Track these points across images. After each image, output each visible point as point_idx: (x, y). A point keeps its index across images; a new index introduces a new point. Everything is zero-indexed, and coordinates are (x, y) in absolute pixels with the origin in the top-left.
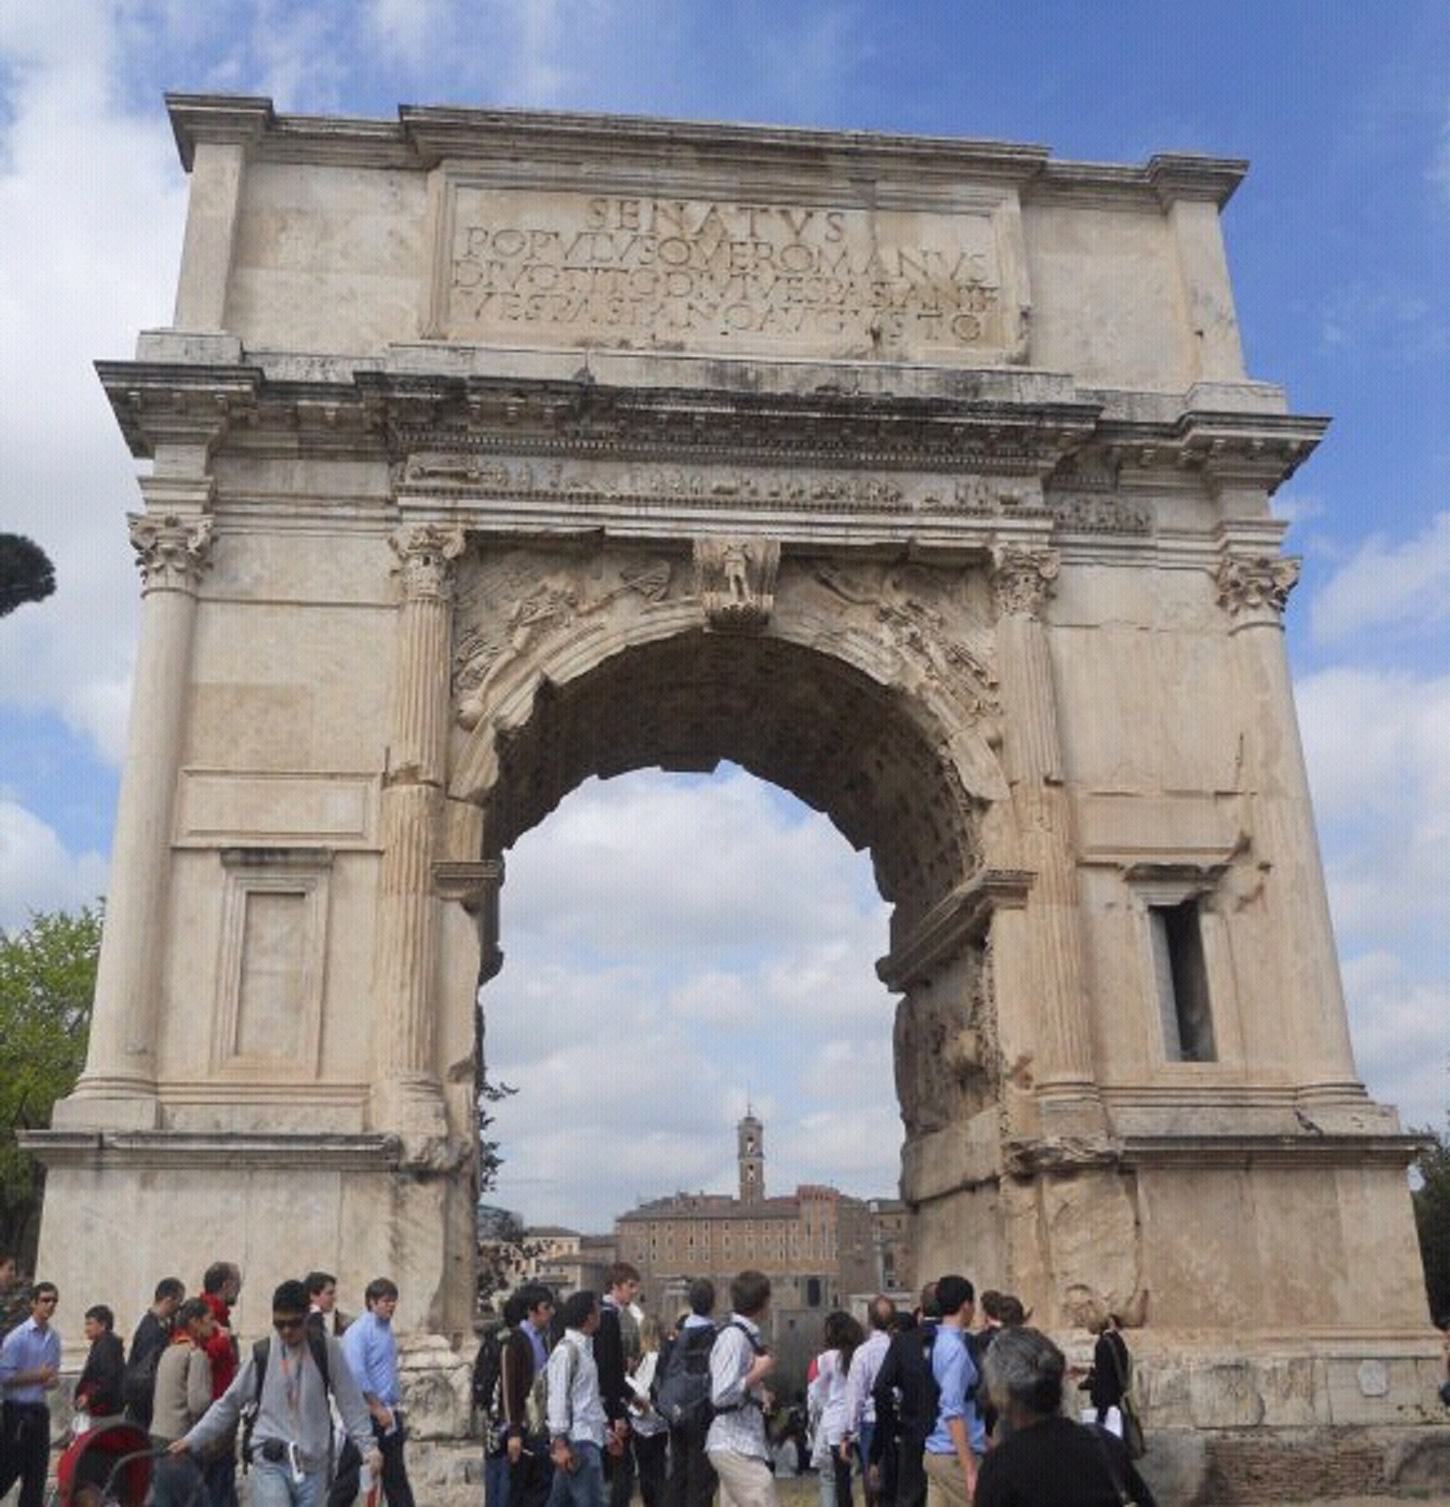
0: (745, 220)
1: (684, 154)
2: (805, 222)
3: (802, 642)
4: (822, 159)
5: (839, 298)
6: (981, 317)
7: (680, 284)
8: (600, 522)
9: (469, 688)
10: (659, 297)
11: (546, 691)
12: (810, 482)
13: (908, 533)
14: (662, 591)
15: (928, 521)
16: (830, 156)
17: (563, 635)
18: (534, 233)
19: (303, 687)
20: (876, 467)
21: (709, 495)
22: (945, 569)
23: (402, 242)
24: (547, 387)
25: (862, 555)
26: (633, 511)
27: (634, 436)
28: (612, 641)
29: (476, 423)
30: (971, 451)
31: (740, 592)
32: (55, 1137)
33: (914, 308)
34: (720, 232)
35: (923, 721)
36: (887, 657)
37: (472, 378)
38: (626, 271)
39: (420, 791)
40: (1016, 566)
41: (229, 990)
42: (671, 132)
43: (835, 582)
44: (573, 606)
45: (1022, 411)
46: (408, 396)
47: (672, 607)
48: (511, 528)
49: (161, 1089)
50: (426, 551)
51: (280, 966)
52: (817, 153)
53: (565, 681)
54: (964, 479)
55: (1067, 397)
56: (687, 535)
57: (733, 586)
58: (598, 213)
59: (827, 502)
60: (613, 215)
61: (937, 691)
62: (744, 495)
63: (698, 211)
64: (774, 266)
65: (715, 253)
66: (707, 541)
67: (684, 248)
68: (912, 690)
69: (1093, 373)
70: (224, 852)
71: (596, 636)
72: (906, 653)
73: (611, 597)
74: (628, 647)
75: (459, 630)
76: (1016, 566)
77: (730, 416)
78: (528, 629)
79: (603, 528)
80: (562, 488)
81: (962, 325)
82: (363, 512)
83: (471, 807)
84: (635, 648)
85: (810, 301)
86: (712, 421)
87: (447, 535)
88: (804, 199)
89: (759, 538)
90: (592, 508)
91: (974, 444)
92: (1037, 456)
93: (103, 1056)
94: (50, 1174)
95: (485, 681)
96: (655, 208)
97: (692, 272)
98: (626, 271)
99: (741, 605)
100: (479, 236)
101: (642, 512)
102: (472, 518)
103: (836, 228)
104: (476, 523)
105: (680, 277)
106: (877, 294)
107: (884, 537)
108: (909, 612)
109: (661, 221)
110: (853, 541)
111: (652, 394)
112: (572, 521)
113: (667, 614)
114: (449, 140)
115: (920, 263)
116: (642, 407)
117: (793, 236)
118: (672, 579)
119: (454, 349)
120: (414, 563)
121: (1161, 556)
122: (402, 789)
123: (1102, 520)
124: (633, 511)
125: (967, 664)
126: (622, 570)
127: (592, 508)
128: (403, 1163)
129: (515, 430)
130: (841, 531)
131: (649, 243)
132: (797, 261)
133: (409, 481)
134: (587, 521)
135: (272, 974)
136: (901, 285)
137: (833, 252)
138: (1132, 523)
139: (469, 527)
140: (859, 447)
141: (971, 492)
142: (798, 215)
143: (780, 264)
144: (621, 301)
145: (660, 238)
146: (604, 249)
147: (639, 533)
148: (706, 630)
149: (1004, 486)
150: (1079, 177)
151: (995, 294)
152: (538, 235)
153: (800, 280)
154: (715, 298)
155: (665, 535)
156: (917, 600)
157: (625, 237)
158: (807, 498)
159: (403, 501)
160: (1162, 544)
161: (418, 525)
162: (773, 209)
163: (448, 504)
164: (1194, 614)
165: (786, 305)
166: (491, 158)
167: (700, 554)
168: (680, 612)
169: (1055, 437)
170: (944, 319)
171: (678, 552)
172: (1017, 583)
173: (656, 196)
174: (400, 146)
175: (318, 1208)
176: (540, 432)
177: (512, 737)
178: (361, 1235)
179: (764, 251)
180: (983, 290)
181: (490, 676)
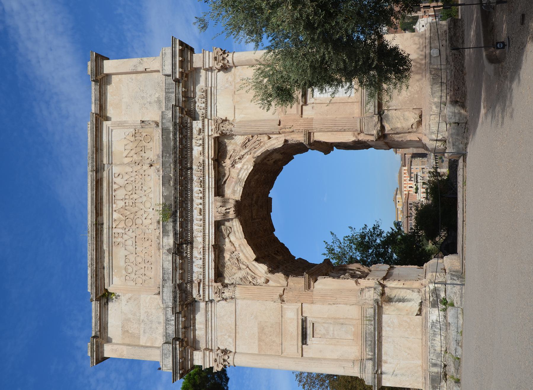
0: (118, 202)
1: (100, 220)
2: (118, 184)
3: (242, 190)
4: (99, 180)
5: (141, 177)
6: (144, 134)
7: (139, 221)
8: (210, 246)
10: (143, 227)
11: (256, 260)
12: (196, 188)
13: (210, 160)
15: (206, 155)
16: (98, 179)
17: (242, 256)
18: (126, 262)
19: (258, 324)
20: (191, 168)
21: (201, 217)
22: (219, 149)
23: (129, 299)
24: (174, 262)
25: (217, 171)
26: (207, 237)
27: (186, 237)
29: (184, 281)
30: (186, 142)
31: (229, 209)
32: (374, 385)
33: (142, 154)
34: (122, 210)
35: (262, 157)
36: (245, 167)
37: (173, 283)
38: (136, 237)
39: (286, 295)
40: (219, 130)
41: (338, 342)
42: (93, 225)
44: (233, 252)
45: (175, 129)
46: (178, 299)
48: (213, 270)
49: (362, 358)
50: (220, 293)
51: (332, 329)
52: (97, 182)
54: (194, 144)
55: (169, 114)
56: (213, 222)
57: (228, 211)
58: (118, 244)
59: (202, 183)
60: (119, 240)
61: (254, 153)
62: (201, 207)
63: (116, 216)
64: (132, 194)
65: (129, 211)
66: (215, 217)
67: (127, 220)
69: (159, 101)
70: (303, 344)
71: (242, 247)
72: (244, 160)
73: (231, 241)
75: (241, 283)
76: (219, 130)
77: (179, 211)
78: (241, 265)
80: (202, 257)
81: (147, 140)
82: (210, 309)
83: (289, 280)
84: (245, 235)
85: (142, 184)
86: (181, 216)
87: (216, 288)
88: (111, 185)
89: (213, 203)
90: (207, 248)
91: (184, 142)
92: (187, 123)
93: (353, 371)
94: (383, 385)
95: (255, 276)
96: (115, 228)
97: (135, 218)
98: (136, 237)
100: (127, 278)
101: (207, 234)
102: (210, 281)
103: (119, 175)
104: (212, 279)
105: (137, 221)
106: (138, 164)
107: (211, 167)
108: (232, 159)
109: (119, 226)
110: (213, 176)
111: (175, 234)
112: (210, 254)
114: (100, 287)
115: (129, 151)
116: (178, 236)
117: (122, 188)
119: (163, 287)
120: (223, 296)
121: (213, 86)
122: (285, 297)
123: (204, 103)
124: (207, 237)
125: (247, 143)
127: (207, 248)
128: (380, 300)
129: (186, 270)
130: (210, 179)
131: (127, 230)
132: (130, 188)
133: (201, 298)
134: (210, 250)
135: (333, 330)
136: (135, 157)
137: (126, 177)
138: (204, 94)
140: (187, 174)
141: (198, 142)
142: (115, 187)
143: (131, 192)
144: (145, 238)
145: (125, 227)
146: (129, 242)
147: (213, 236)
149: (195, 132)
150: (98, 103)
151: (137, 130)
152: (126, 261)
153: (135, 187)
154: (143, 211)
155: (213, 228)
156: (228, 156)
157: (125, 237)
158: (201, 189)
159: (207, 299)
160: (210, 86)
161: (213, 295)
162: (114, 194)
163: (207, 287)
164: (230, 77)
165: (143, 191)
166: (104, 275)
167: (219, 219)
169: (181, 118)
170: (145, 145)
171: (218, 225)
172: (223, 130)
173: (112, 228)
174: (102, 300)
175: (391, 320)
176: (186, 263)
178: (398, 309)
179: (127, 197)
180: (135, 133)
181: (253, 275)
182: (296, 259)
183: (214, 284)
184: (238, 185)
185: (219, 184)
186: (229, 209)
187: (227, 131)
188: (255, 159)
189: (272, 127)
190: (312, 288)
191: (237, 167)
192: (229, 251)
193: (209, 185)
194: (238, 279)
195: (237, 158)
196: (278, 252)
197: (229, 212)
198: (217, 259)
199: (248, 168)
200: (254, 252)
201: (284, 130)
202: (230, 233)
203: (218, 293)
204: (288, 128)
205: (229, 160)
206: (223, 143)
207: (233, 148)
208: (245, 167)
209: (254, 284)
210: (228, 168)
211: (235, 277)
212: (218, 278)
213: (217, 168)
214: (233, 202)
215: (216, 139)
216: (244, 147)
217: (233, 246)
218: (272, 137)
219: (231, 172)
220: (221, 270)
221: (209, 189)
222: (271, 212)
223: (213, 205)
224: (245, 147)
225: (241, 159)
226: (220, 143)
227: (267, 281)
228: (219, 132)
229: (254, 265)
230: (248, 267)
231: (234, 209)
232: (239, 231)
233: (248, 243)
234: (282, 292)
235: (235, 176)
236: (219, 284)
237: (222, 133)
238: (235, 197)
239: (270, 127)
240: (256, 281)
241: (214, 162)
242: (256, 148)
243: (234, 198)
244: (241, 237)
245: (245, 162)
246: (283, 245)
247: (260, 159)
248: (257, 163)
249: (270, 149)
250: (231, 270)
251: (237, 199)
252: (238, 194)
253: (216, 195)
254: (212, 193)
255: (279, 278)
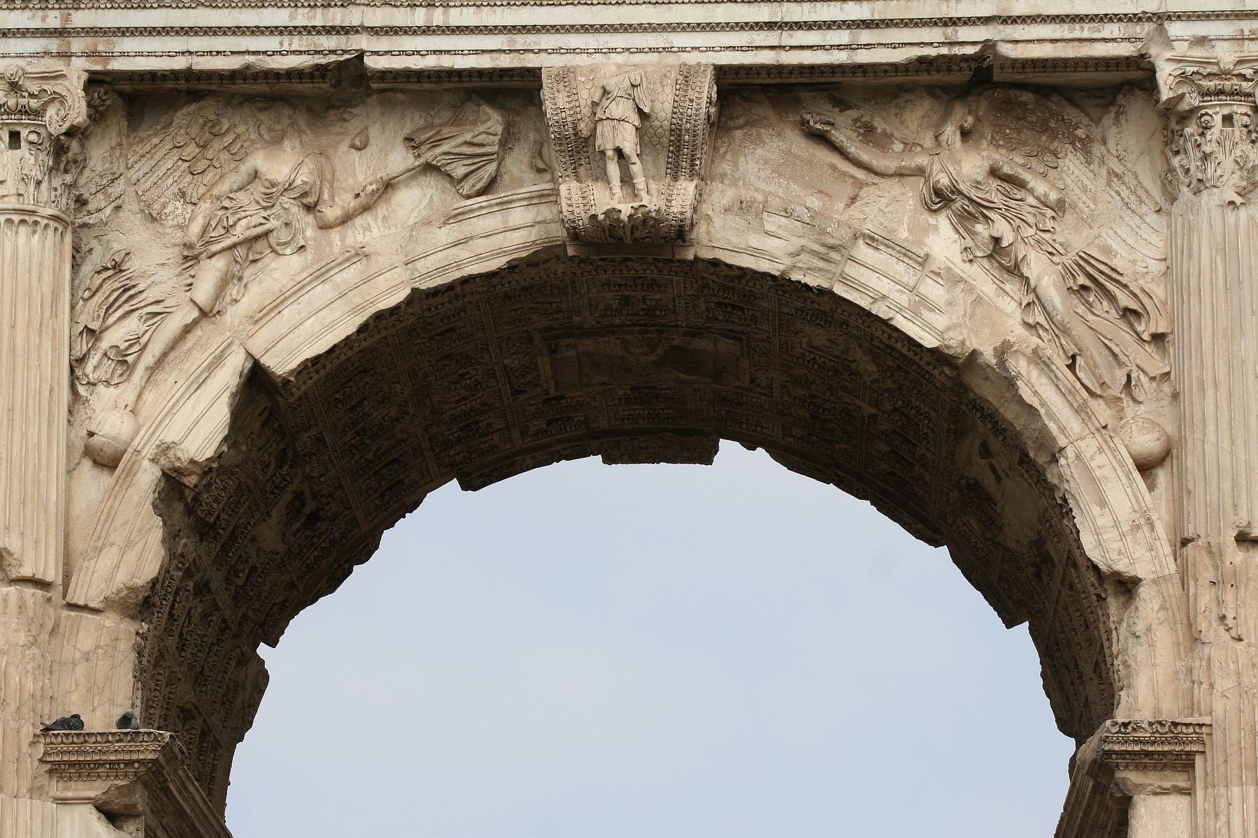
3: (763, 266)
9: (107, 383)
13: (980, 33)
14: (492, 168)
25: (900, 79)
28: (383, 282)
31: (627, 180)
35: (1009, 413)
36: (934, 291)
40: (1205, 93)
43: (838, 136)
44: (309, 208)
47: (504, 205)
48: (179, 63)
50: (13, 119)
53: (294, 364)
56: (531, 61)
57: (613, 170)
61: (1037, 358)
66: (565, 75)
68: (989, 356)
71: (351, 274)
72: (982, 278)
73: (389, 186)
74: (414, 290)
75: (87, 268)
76: (1205, 93)
78: (219, 263)
79: (361, 55)
83: (110, 621)
84: (435, 292)
89: (672, 59)
99: (626, 210)
102: (102, 45)
104: (111, 56)
108: (993, 192)
110: (863, 57)
112: (297, 43)
113: (491, 222)
118: (507, 142)
125: (1111, 298)
126: (407, 131)
130: (843, 37)
139: (98, 68)
147: (430, 62)
148: (571, 252)
155: (485, 62)
156: (1012, 163)
167: (555, 101)
168: (519, 215)
177: (191, 481)
181: (149, 358)
182: (263, 650)
183: (77, 71)
184: (797, 243)
185: (803, 95)
186: (627, 180)
187: (1194, 155)
188: (993, 361)
189: (1227, 486)
190: (56, 788)
191: (936, 228)
192: (322, 178)
193: (799, 26)
194: (118, 244)
195: (1001, 228)
196: (314, 518)
197: (603, 177)
198: (261, 88)
199: (926, 314)
200: (316, 360)
201: (1207, 575)
202: (456, 182)
203: (12, 102)
204: (1220, 603)
205: (986, 165)
206: (1108, 120)
207: (1074, 194)
208: (934, 291)
209: (82, 360)
210: (921, 160)
211: (131, 218)
212: (121, 94)
213: (923, 78)
214: (676, 208)
215: (1135, 75)
216: (1082, 280)
217: (353, 204)
218: (1151, 487)
219: (893, 188)
220: (180, 117)
221: (770, 26)
222: (608, 460)
223: (654, 57)
224: (1083, 287)
225: (990, 257)
226: (1112, 102)
227: (107, 461)
228: (1193, 100)
229: (219, 360)
230: (204, 314)
231: (624, 216)
232: (462, 253)
233: (379, 316)
234: (27, 571)
235: (871, 211)
236: (78, 111)
237: (1184, 117)
238: (718, 221)
239: (1227, 476)
240: (102, 374)
241: (965, 58)
242: (1072, 367)
243: (706, 208)
244: (419, 265)
245: (971, 289)
246: (364, 549)
247: (987, 392)
248: (966, 378)
249: (1065, 471)
250: (183, 195)
251: (700, 232)
252: (736, 240)
253: (730, 79)
254: (741, 49)
255: (129, 545)
